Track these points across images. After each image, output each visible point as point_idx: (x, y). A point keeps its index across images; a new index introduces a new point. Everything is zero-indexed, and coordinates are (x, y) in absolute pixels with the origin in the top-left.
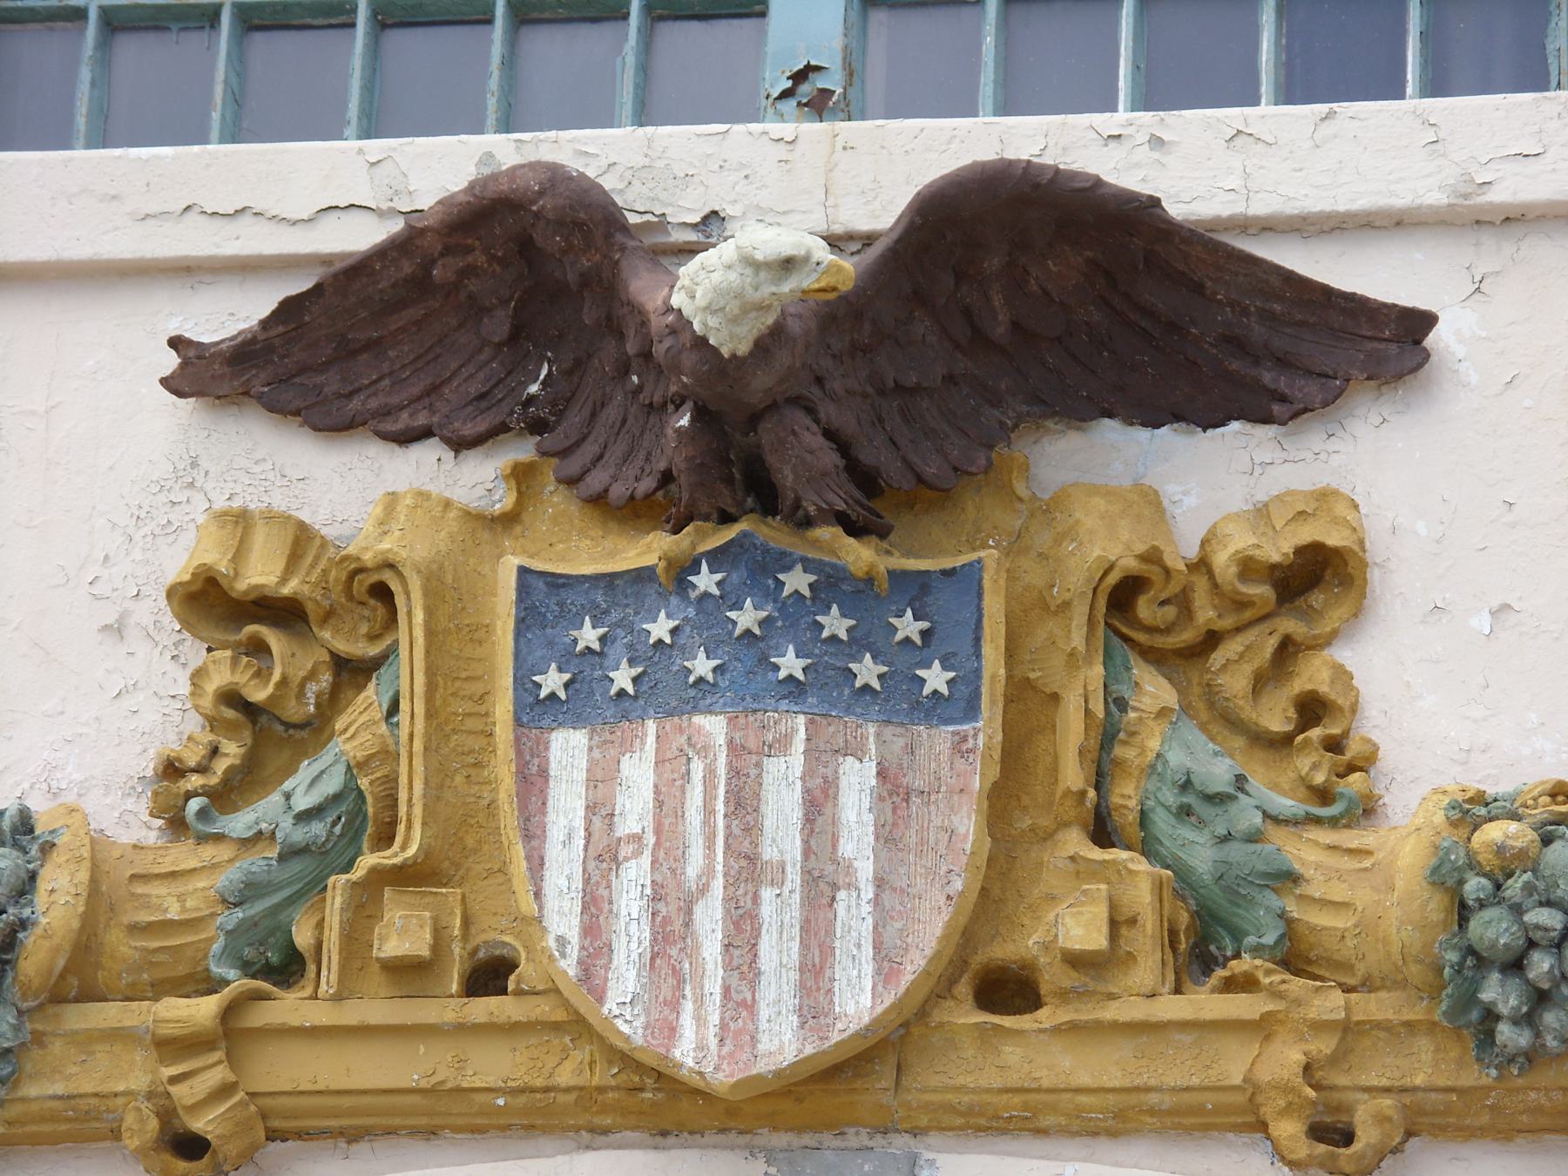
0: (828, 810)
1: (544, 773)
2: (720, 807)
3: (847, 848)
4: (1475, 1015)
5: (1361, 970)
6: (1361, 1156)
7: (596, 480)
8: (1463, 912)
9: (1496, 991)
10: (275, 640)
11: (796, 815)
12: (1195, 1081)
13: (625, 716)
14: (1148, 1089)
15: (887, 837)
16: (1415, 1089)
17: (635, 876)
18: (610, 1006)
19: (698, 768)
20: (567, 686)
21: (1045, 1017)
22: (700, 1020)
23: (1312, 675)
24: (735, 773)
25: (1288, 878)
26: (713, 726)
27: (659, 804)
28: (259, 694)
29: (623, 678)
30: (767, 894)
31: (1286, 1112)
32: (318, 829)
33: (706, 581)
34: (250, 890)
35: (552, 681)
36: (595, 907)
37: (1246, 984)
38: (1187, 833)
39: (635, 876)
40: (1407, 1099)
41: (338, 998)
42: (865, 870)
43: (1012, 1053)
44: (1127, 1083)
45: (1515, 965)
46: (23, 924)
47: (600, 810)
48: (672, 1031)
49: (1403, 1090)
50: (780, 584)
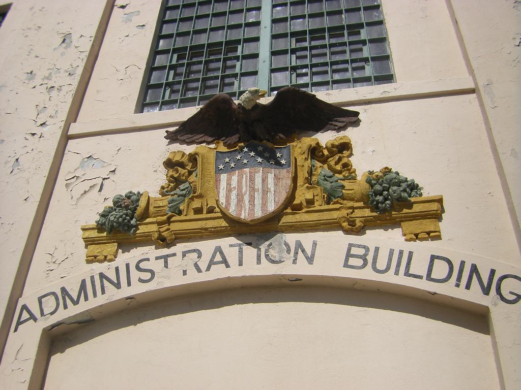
0: (266, 181)
1: (220, 180)
2: (248, 181)
3: (269, 186)
4: (375, 203)
5: (356, 199)
6: (357, 228)
7: (229, 142)
8: (372, 186)
9: (380, 198)
10: (179, 168)
11: (261, 182)
12: (329, 218)
13: (233, 171)
14: (321, 220)
15: (276, 185)
16: (366, 217)
17: (234, 194)
18: (230, 211)
19: (244, 176)
20: (224, 167)
21: (304, 211)
22: (245, 213)
23: (345, 160)
24: (250, 176)
25: (343, 187)
26: (247, 170)
27: (238, 182)
28: (176, 176)
29: (233, 165)
30: (256, 193)
31: (344, 222)
32: (184, 192)
33: (246, 150)
34: (173, 201)
35: (221, 167)
36: (228, 198)
37: (337, 203)
38: (325, 182)
39: (234, 194)
40: (364, 218)
41: (186, 215)
42: (272, 189)
43: (297, 216)
44: (317, 219)
45: (381, 194)
46: (138, 206)
47: (229, 184)
48: (241, 214)
49: (364, 217)
50: (258, 149)
